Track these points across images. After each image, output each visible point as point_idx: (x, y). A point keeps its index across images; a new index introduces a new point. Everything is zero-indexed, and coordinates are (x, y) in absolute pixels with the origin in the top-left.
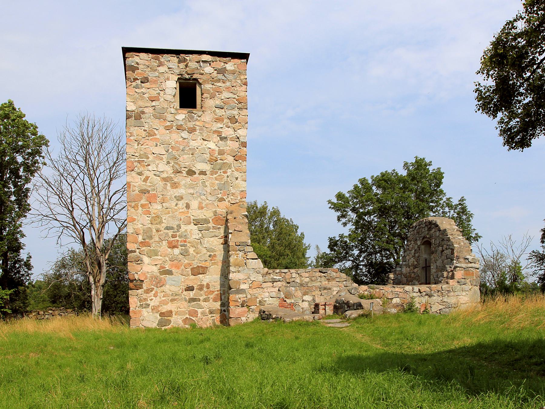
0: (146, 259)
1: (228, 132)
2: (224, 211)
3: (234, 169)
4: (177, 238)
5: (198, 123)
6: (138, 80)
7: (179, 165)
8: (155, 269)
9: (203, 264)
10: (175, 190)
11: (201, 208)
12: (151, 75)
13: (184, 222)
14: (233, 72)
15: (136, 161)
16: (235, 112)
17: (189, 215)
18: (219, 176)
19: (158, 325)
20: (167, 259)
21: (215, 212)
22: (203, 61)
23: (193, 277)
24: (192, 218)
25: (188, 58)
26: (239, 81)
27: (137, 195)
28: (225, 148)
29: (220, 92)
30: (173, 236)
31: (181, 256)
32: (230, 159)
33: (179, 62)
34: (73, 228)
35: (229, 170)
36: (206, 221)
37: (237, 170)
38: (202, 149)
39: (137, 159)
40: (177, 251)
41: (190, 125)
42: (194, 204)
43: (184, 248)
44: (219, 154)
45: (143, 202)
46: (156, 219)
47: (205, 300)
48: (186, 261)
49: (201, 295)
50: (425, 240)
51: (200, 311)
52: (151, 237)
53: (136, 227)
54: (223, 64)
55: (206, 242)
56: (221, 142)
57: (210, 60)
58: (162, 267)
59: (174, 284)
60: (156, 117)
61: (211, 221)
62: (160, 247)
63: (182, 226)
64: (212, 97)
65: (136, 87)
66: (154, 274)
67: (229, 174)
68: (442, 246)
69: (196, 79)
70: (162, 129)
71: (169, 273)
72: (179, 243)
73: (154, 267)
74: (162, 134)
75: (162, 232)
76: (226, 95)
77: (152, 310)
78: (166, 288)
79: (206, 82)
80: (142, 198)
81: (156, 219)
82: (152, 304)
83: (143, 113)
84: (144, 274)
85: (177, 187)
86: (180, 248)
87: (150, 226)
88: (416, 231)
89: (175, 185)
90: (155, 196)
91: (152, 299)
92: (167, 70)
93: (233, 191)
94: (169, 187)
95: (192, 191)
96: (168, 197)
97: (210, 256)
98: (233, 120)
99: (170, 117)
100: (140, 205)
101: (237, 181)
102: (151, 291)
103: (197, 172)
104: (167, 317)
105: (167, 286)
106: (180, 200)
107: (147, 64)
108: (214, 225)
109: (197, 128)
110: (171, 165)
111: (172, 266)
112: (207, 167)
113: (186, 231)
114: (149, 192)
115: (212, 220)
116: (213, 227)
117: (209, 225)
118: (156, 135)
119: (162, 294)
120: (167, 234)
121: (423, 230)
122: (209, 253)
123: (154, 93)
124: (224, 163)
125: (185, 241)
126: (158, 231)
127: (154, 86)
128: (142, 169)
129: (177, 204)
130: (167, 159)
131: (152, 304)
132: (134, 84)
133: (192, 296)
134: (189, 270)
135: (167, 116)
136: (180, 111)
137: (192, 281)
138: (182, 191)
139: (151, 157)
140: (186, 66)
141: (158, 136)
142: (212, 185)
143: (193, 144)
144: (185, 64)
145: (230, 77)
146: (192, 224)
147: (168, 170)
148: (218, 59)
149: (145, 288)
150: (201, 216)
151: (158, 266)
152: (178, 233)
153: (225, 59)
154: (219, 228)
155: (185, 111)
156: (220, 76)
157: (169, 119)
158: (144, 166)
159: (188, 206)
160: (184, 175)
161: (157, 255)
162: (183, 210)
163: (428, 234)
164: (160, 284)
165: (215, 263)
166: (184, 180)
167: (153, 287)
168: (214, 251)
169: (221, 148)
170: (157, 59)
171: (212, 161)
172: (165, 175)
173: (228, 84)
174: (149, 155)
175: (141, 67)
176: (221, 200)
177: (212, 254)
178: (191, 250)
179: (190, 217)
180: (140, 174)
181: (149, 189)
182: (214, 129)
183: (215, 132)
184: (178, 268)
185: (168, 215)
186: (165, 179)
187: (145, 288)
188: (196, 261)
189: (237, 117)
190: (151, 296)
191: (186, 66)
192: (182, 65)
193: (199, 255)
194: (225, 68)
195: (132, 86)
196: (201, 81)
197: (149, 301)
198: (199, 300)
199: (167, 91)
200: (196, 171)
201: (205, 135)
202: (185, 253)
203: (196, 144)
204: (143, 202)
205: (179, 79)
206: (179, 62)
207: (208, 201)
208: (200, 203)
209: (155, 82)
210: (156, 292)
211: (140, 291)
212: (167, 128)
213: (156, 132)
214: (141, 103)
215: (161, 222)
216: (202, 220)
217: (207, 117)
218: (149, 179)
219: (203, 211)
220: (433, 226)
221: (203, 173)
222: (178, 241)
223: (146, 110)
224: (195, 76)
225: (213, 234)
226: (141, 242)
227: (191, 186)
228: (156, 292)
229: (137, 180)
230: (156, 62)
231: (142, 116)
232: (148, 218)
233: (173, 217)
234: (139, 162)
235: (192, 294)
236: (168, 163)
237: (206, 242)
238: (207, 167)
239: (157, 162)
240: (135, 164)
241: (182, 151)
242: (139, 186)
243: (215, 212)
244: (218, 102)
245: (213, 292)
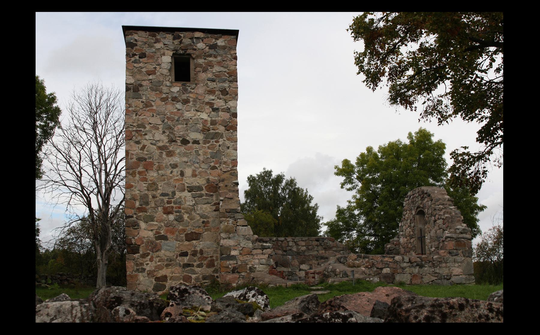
0: (143, 225)
1: (219, 103)
2: (216, 178)
3: (225, 139)
4: (172, 205)
5: (191, 95)
6: (137, 55)
7: (174, 135)
8: (151, 234)
9: (196, 230)
10: (170, 158)
11: (194, 175)
12: (148, 51)
13: (178, 189)
14: (224, 48)
15: (134, 131)
16: (226, 85)
17: (183, 182)
18: (211, 145)
19: (153, 289)
20: (163, 224)
21: (208, 180)
22: (196, 38)
23: (187, 243)
24: (186, 185)
25: (182, 35)
26: (229, 56)
27: (134, 162)
28: (217, 119)
29: (212, 67)
30: (169, 202)
31: (175, 222)
32: (221, 129)
33: (174, 39)
34: (81, 193)
35: (221, 140)
36: (200, 188)
37: (228, 139)
38: (195, 119)
39: (135, 129)
40: (171, 217)
41: (184, 97)
42: (188, 172)
43: (178, 214)
44: (211, 124)
45: (141, 169)
46: (153, 186)
47: (199, 266)
48: (181, 227)
49: (195, 261)
50: (419, 209)
51: (194, 276)
52: (147, 203)
53: (133, 193)
54: (214, 40)
55: (199, 208)
56: (213, 113)
57: (202, 36)
58: (157, 233)
59: (169, 249)
60: (152, 90)
61: (204, 188)
62: (156, 212)
63: (177, 192)
64: (205, 71)
65: (135, 62)
66: (150, 239)
67: (221, 143)
68: (435, 216)
69: (190, 55)
70: (159, 102)
71: (165, 238)
72: (174, 210)
73: (150, 232)
74: (157, 105)
75: (158, 199)
76: (217, 69)
77: (148, 274)
78: (162, 253)
79: (198, 57)
80: (139, 166)
81: (153, 186)
82: (148, 268)
83: (141, 85)
84: (141, 239)
85: (172, 156)
86: (175, 214)
87: (146, 192)
88: (410, 201)
89: (170, 154)
90: (152, 164)
91: (147, 264)
92: (163, 46)
93: (225, 160)
94: (164, 156)
95: (185, 159)
96: (164, 165)
97: (203, 222)
98: (224, 92)
99: (165, 89)
100: (137, 172)
101: (228, 150)
102: (147, 256)
103: (191, 141)
104: (162, 282)
105: (163, 251)
106: (175, 168)
107: (145, 41)
108: (207, 192)
109: (191, 99)
110: (167, 134)
111: (167, 231)
112: (199, 137)
113: (180, 197)
114: (145, 159)
115: (206, 187)
116: (206, 194)
117: (203, 192)
118: (152, 106)
119: (158, 259)
120: (163, 200)
121: (417, 200)
122: (202, 220)
123: (151, 67)
124: (216, 133)
125: (180, 208)
126: (154, 197)
127: (151, 61)
128: (139, 138)
129: (172, 172)
130: (163, 129)
131: (148, 268)
132: (133, 59)
133: (186, 262)
134: (183, 235)
135: (164, 88)
136: (174, 84)
137: (186, 246)
138: (176, 159)
139: (148, 127)
140: (181, 42)
141: (154, 108)
142: (205, 153)
143: (187, 115)
144: (179, 40)
145: (221, 52)
146: (186, 191)
147: (163, 139)
148: (209, 36)
149: (141, 253)
150: (195, 184)
151: (154, 232)
152: (173, 200)
153: (216, 36)
154: (212, 195)
155: (179, 84)
156: (212, 52)
157: (165, 91)
158: (141, 135)
159: (182, 174)
160: (179, 144)
161: (153, 221)
162: (177, 178)
163: (421, 204)
164: (156, 248)
165: (208, 229)
166: (179, 149)
167: (149, 251)
168: (206, 217)
169: (213, 119)
170: (154, 36)
171: (205, 130)
172: (160, 144)
173: (219, 58)
174: (146, 125)
175: (139, 43)
176: (214, 168)
177: (205, 220)
178: (186, 217)
179: (184, 184)
180: (138, 142)
181: (146, 157)
182: (207, 100)
183: (207, 103)
184: (173, 234)
185: (163, 182)
186: (160, 148)
187: (141, 253)
188: (190, 227)
189: (228, 90)
190: (147, 261)
191: (181, 42)
192: (176, 42)
193: (193, 221)
194: (217, 43)
195: (131, 61)
196: (194, 56)
197: (145, 266)
198: (193, 266)
199: (163, 65)
200: (190, 140)
201: (198, 106)
202: (180, 219)
203: (190, 115)
204: (141, 169)
205: (173, 54)
206: (174, 39)
207: (201, 169)
208: (194, 171)
209: (152, 57)
210: (152, 257)
211: (136, 255)
212: (163, 100)
213: (153, 104)
214: (138, 77)
215: (157, 189)
216: (196, 187)
217: (200, 90)
218: (146, 147)
219: (197, 178)
220: (425, 195)
221: (196, 142)
222: (172, 207)
223: (144, 83)
224: (189, 51)
225: (206, 201)
226: (138, 208)
227: (185, 155)
228: (152, 257)
229: (135, 149)
230: (153, 39)
231: (140, 88)
232: (145, 185)
233: (169, 184)
234: (137, 131)
235: (186, 260)
236: (164, 132)
237: (199, 208)
238: (199, 137)
239: (154, 131)
240: (134, 133)
241: (177, 121)
242: (137, 154)
243: (208, 180)
244: (210, 75)
245: (207, 258)
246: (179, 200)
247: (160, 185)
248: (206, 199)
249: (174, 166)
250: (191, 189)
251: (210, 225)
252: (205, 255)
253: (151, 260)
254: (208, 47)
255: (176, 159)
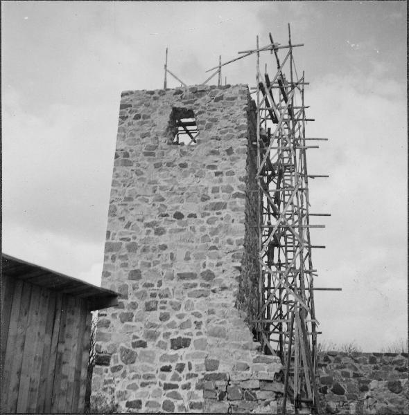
11: (187, 259)
36: (193, 276)
38: (193, 187)
42: (180, 254)
47: (186, 387)
49: (180, 380)
71: (143, 345)
76: (224, 123)
85: (162, 234)
89: (160, 232)
94: (152, 235)
103: (186, 215)
106: (164, 249)
114: (129, 240)
131: (118, 389)
150: (187, 270)
161: (131, 320)
164: (129, 358)
172: (149, 220)
180: (122, 219)
181: (131, 237)
186: (148, 225)
200: (184, 214)
210: (125, 372)
213: (144, 171)
222: (157, 302)
225: (201, 293)
228: (125, 372)
245: (196, 376)
246: (165, 293)
247: (144, 271)
248: (200, 290)
249: (164, 247)
250: (182, 277)
251: (203, 326)
252: (193, 371)
253: (124, 375)
254: (213, 101)
255: (163, 240)
